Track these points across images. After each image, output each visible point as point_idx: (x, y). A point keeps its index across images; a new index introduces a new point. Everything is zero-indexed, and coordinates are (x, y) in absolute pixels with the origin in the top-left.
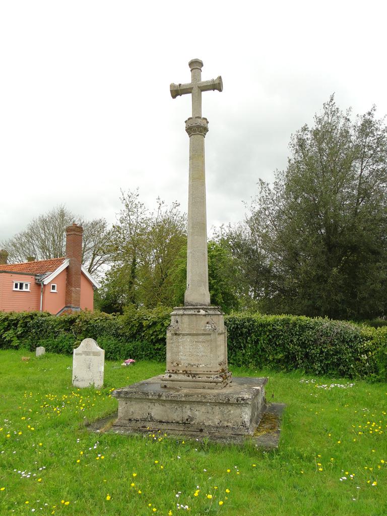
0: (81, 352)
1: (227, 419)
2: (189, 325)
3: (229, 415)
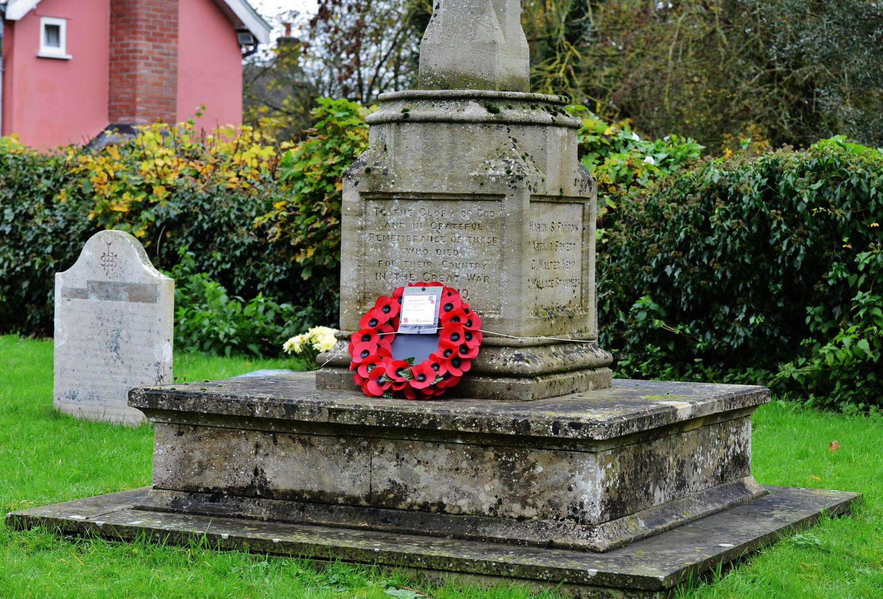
0: (82, 285)
1: (522, 493)
2: (425, 160)
3: (528, 483)
